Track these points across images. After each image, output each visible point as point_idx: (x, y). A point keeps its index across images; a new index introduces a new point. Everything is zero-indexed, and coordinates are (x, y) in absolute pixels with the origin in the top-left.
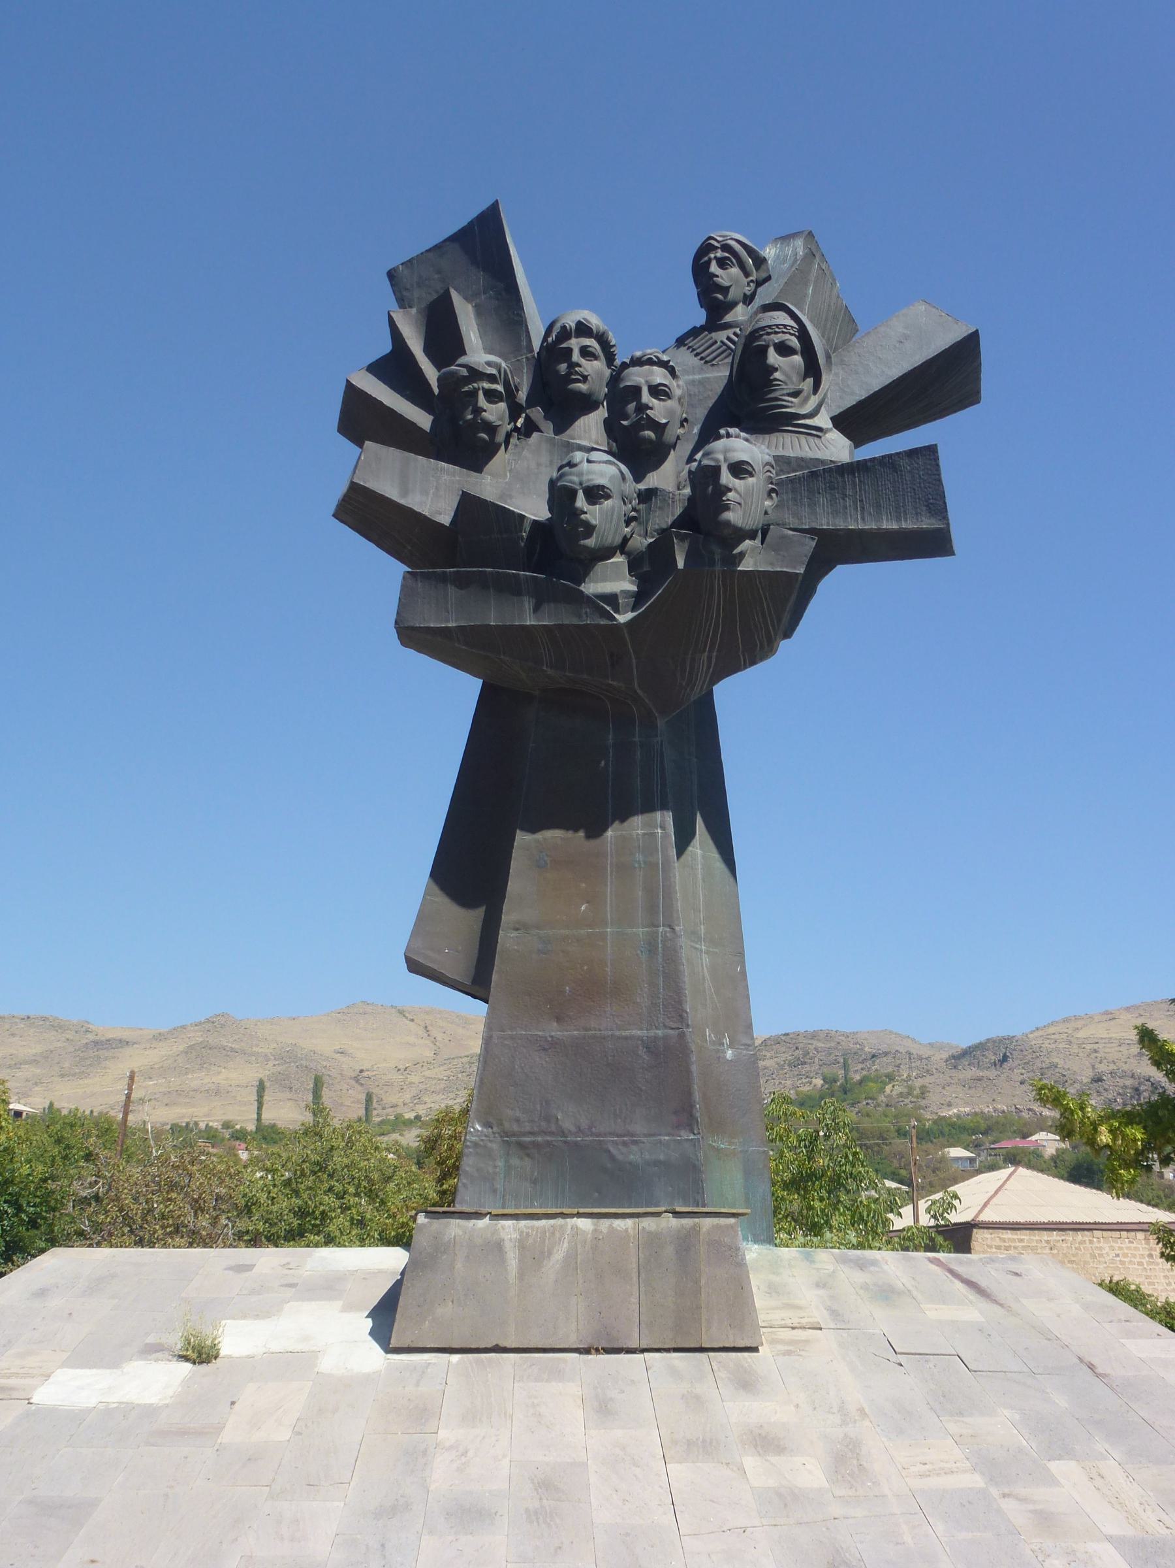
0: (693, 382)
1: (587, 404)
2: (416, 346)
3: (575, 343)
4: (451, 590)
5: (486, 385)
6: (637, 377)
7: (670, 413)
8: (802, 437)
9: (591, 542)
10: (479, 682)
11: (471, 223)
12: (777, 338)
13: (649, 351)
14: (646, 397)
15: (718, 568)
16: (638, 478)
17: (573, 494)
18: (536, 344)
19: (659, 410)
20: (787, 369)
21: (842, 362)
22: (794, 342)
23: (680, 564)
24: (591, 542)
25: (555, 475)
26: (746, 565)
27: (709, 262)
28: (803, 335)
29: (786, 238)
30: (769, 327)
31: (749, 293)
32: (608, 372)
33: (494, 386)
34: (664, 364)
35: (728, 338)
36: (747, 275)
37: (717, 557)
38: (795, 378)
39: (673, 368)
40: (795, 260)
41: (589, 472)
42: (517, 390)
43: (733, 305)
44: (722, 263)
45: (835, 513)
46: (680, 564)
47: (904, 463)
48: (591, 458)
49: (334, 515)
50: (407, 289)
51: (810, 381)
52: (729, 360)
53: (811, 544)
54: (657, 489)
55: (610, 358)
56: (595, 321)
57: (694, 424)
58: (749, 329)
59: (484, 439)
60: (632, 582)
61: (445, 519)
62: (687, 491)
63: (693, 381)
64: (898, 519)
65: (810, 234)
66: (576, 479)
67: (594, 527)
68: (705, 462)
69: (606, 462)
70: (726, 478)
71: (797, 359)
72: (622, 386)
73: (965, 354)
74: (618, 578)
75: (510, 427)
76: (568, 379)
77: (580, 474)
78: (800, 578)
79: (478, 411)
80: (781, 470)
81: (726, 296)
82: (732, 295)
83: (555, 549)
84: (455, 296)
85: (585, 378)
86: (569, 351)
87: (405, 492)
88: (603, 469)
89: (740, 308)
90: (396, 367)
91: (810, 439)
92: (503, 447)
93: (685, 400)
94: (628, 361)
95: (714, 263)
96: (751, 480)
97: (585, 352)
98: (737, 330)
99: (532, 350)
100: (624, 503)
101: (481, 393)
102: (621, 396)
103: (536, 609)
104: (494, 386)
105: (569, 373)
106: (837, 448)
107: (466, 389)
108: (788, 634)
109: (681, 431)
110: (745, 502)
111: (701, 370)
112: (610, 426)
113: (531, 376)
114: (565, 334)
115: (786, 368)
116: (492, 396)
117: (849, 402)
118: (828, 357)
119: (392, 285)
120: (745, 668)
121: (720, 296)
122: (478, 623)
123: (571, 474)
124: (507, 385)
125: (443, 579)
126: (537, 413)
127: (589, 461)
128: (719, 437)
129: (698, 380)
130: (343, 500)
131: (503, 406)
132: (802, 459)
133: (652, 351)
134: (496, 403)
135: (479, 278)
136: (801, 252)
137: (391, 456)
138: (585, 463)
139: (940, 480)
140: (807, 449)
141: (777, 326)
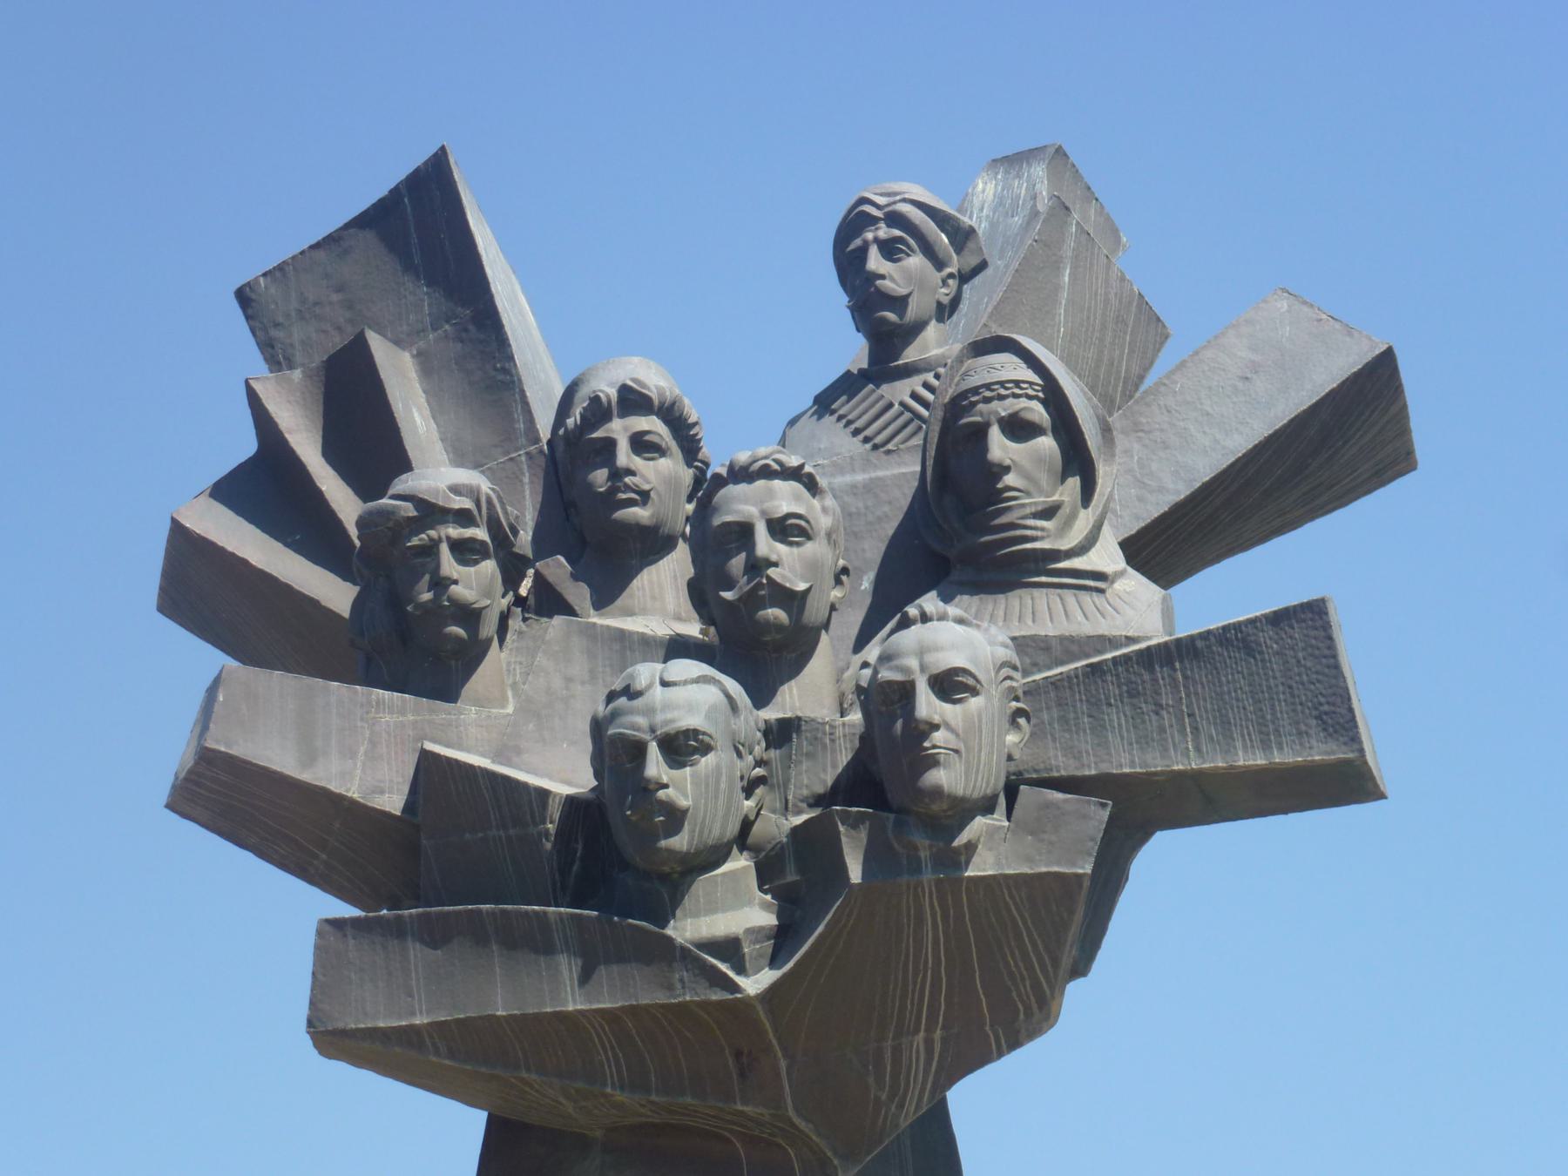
0: (853, 489)
1: (654, 543)
2: (307, 446)
3: (619, 429)
4: (416, 952)
5: (454, 532)
6: (741, 503)
7: (813, 567)
8: (1069, 595)
9: (680, 842)
10: (482, 1116)
11: (395, 192)
12: (1003, 409)
13: (762, 451)
14: (764, 544)
15: (928, 877)
16: (761, 697)
17: (637, 751)
18: (544, 424)
19: (790, 565)
20: (1026, 464)
21: (1137, 428)
22: (1038, 412)
23: (855, 874)
24: (680, 842)
25: (601, 710)
26: (981, 867)
27: (863, 251)
28: (1054, 397)
29: (1014, 161)
30: (988, 386)
31: (946, 300)
32: (687, 475)
33: (469, 532)
34: (795, 474)
35: (915, 396)
36: (939, 264)
37: (924, 854)
38: (1044, 479)
39: (810, 476)
40: (1035, 213)
41: (667, 706)
42: (515, 532)
43: (918, 328)
44: (890, 250)
45: (1144, 741)
46: (855, 874)
47: (1266, 636)
48: (669, 678)
49: (171, 806)
50: (277, 325)
51: (1074, 483)
52: (918, 441)
53: (1097, 815)
54: (799, 719)
55: (690, 448)
56: (655, 380)
57: (861, 572)
58: (951, 392)
59: (458, 638)
60: (765, 906)
61: (393, 802)
62: (856, 717)
63: (854, 486)
64: (1266, 746)
65: (1060, 152)
66: (641, 721)
67: (684, 813)
68: (886, 674)
69: (697, 680)
70: (927, 704)
71: (1046, 443)
72: (717, 521)
73: (1377, 383)
74: (739, 901)
75: (505, 602)
76: (610, 501)
77: (649, 711)
78: (1086, 883)
79: (441, 584)
80: (1035, 664)
81: (901, 314)
82: (912, 312)
83: (610, 856)
84: (378, 345)
85: (645, 496)
86: (610, 444)
87: (310, 758)
88: (693, 695)
89: (932, 331)
90: (266, 485)
91: (1086, 597)
92: (495, 643)
93: (841, 538)
94: (723, 471)
95: (874, 252)
96: (975, 703)
97: (640, 444)
98: (930, 377)
99: (537, 440)
100: (739, 755)
101: (444, 549)
102: (719, 544)
103: (585, 977)
104: (469, 532)
105: (613, 491)
106: (1138, 611)
107: (415, 541)
108: (1080, 968)
109: (836, 593)
110: (967, 746)
111: (867, 464)
112: (700, 594)
113: (540, 489)
114: (598, 412)
115: (1023, 462)
116: (466, 551)
117: (1155, 507)
118: (1106, 430)
119: (248, 318)
120: (1000, 1055)
121: (891, 316)
122: (472, 1013)
123: (631, 712)
124: (494, 526)
125: (397, 930)
126: (557, 568)
127: (665, 684)
128: (906, 623)
129: (861, 487)
130: (186, 779)
131: (489, 566)
132: (1071, 639)
133: (765, 450)
134: (476, 562)
135: (421, 299)
136: (1043, 190)
137: (278, 685)
138: (658, 689)
139: (1337, 667)
140: (1080, 617)
141: (1002, 384)
